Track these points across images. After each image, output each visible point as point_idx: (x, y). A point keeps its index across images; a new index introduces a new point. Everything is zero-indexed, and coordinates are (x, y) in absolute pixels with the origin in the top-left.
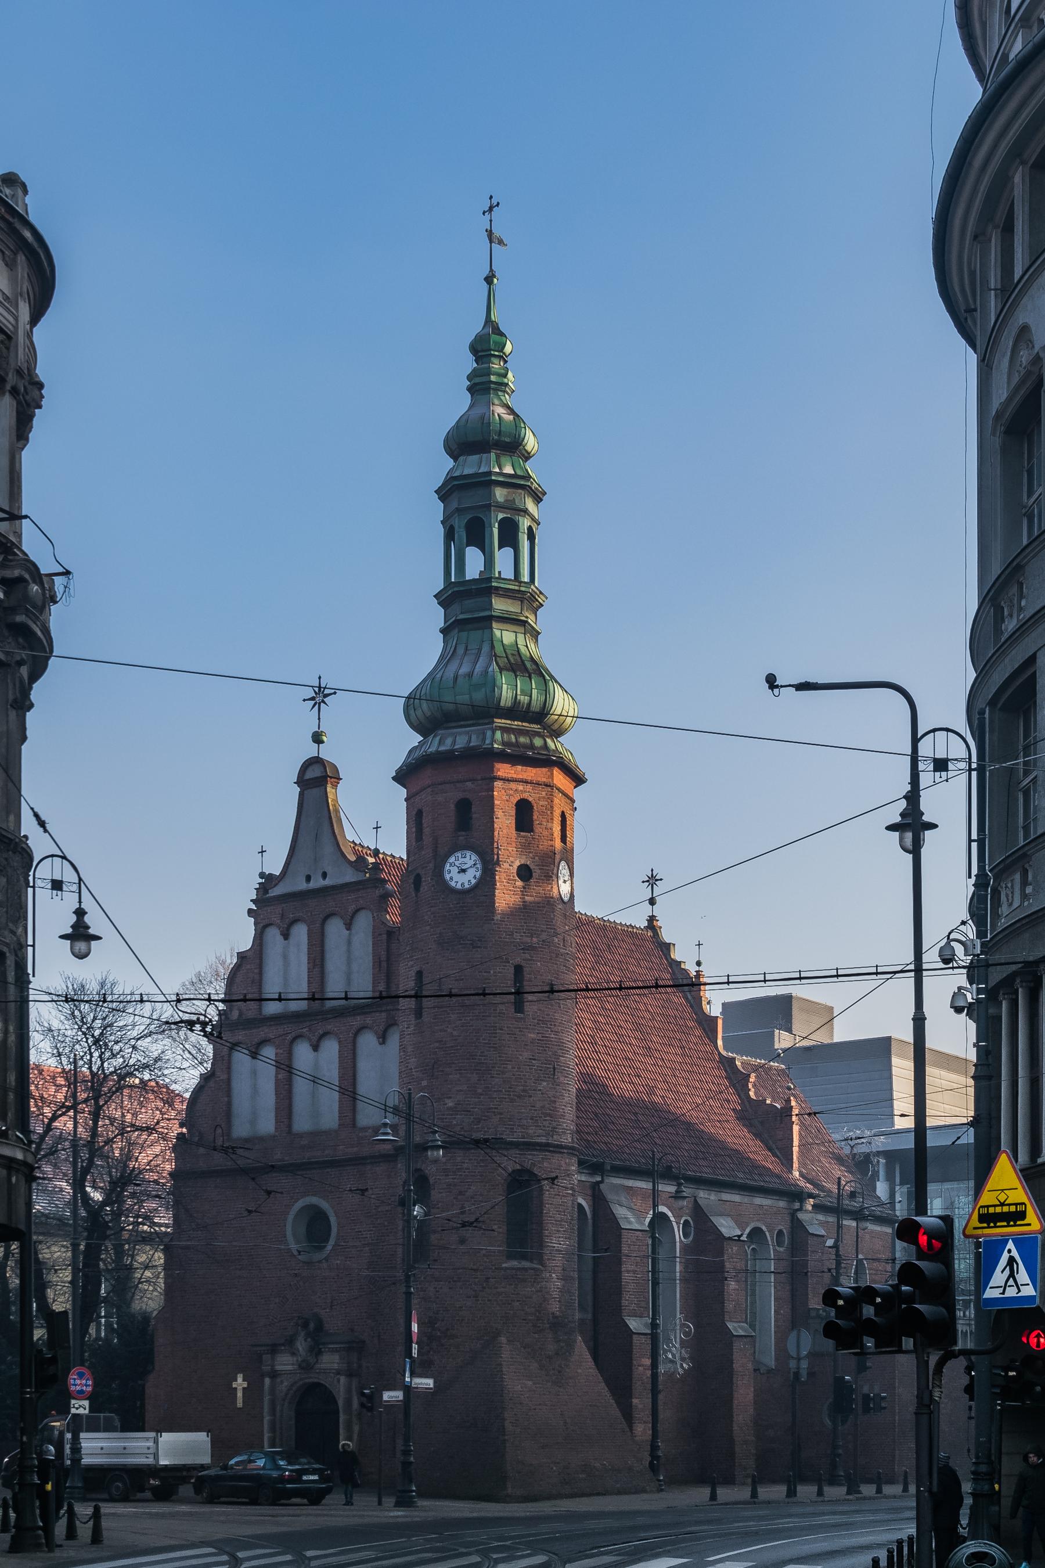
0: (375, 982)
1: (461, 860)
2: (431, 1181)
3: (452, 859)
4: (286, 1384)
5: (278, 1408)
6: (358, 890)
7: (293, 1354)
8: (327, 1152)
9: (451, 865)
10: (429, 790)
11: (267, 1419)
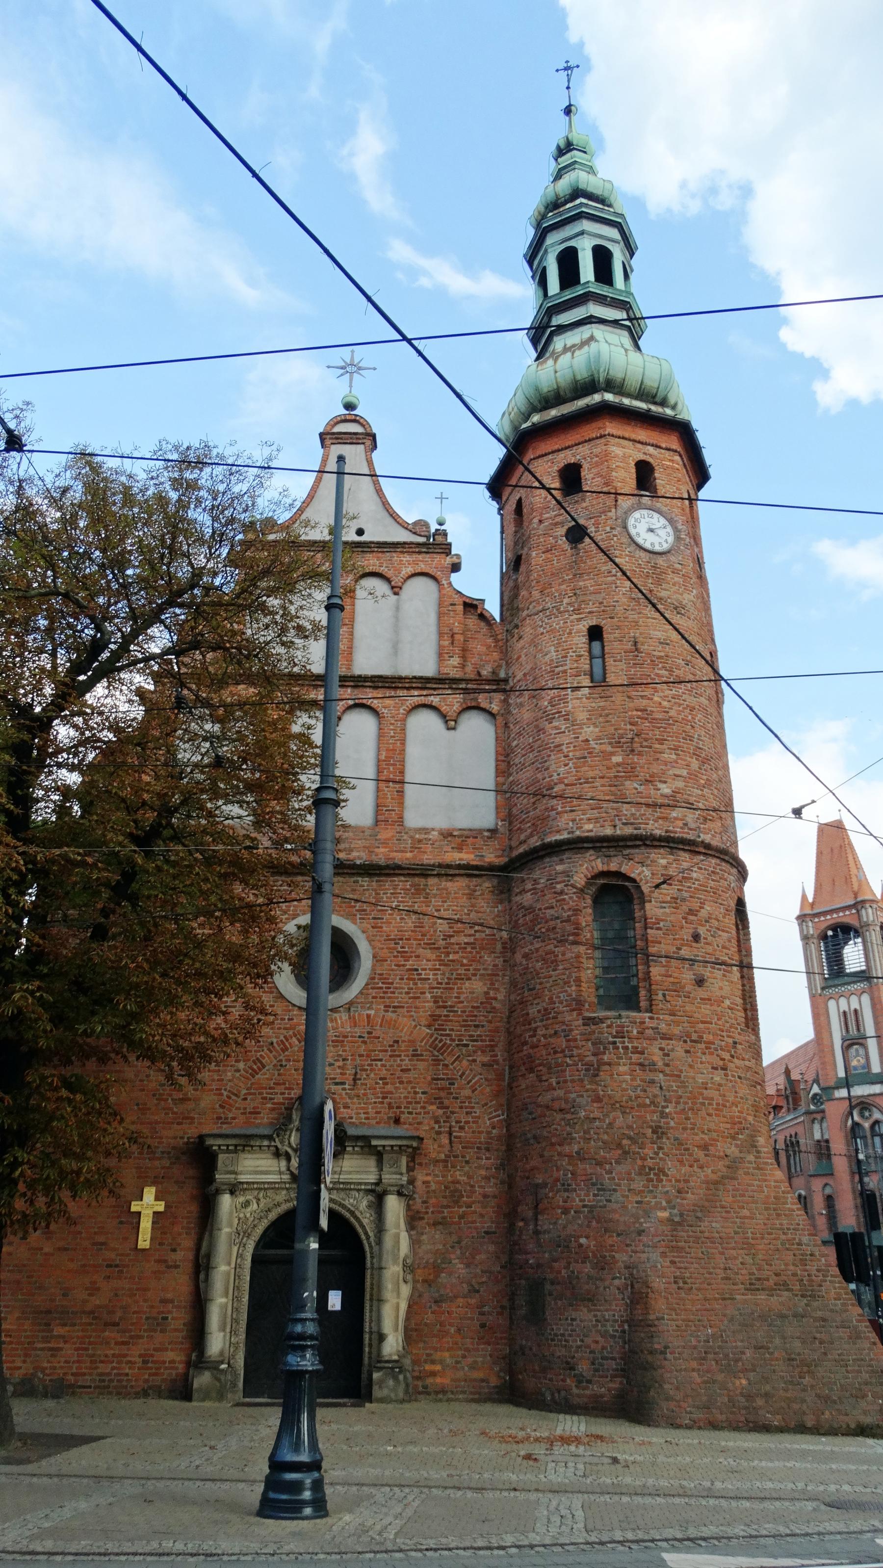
0: (441, 655)
1: (647, 519)
3: (637, 514)
6: (420, 553)
7: (277, 1154)
8: (355, 854)
9: (636, 520)
10: (603, 440)
11: (223, 1268)
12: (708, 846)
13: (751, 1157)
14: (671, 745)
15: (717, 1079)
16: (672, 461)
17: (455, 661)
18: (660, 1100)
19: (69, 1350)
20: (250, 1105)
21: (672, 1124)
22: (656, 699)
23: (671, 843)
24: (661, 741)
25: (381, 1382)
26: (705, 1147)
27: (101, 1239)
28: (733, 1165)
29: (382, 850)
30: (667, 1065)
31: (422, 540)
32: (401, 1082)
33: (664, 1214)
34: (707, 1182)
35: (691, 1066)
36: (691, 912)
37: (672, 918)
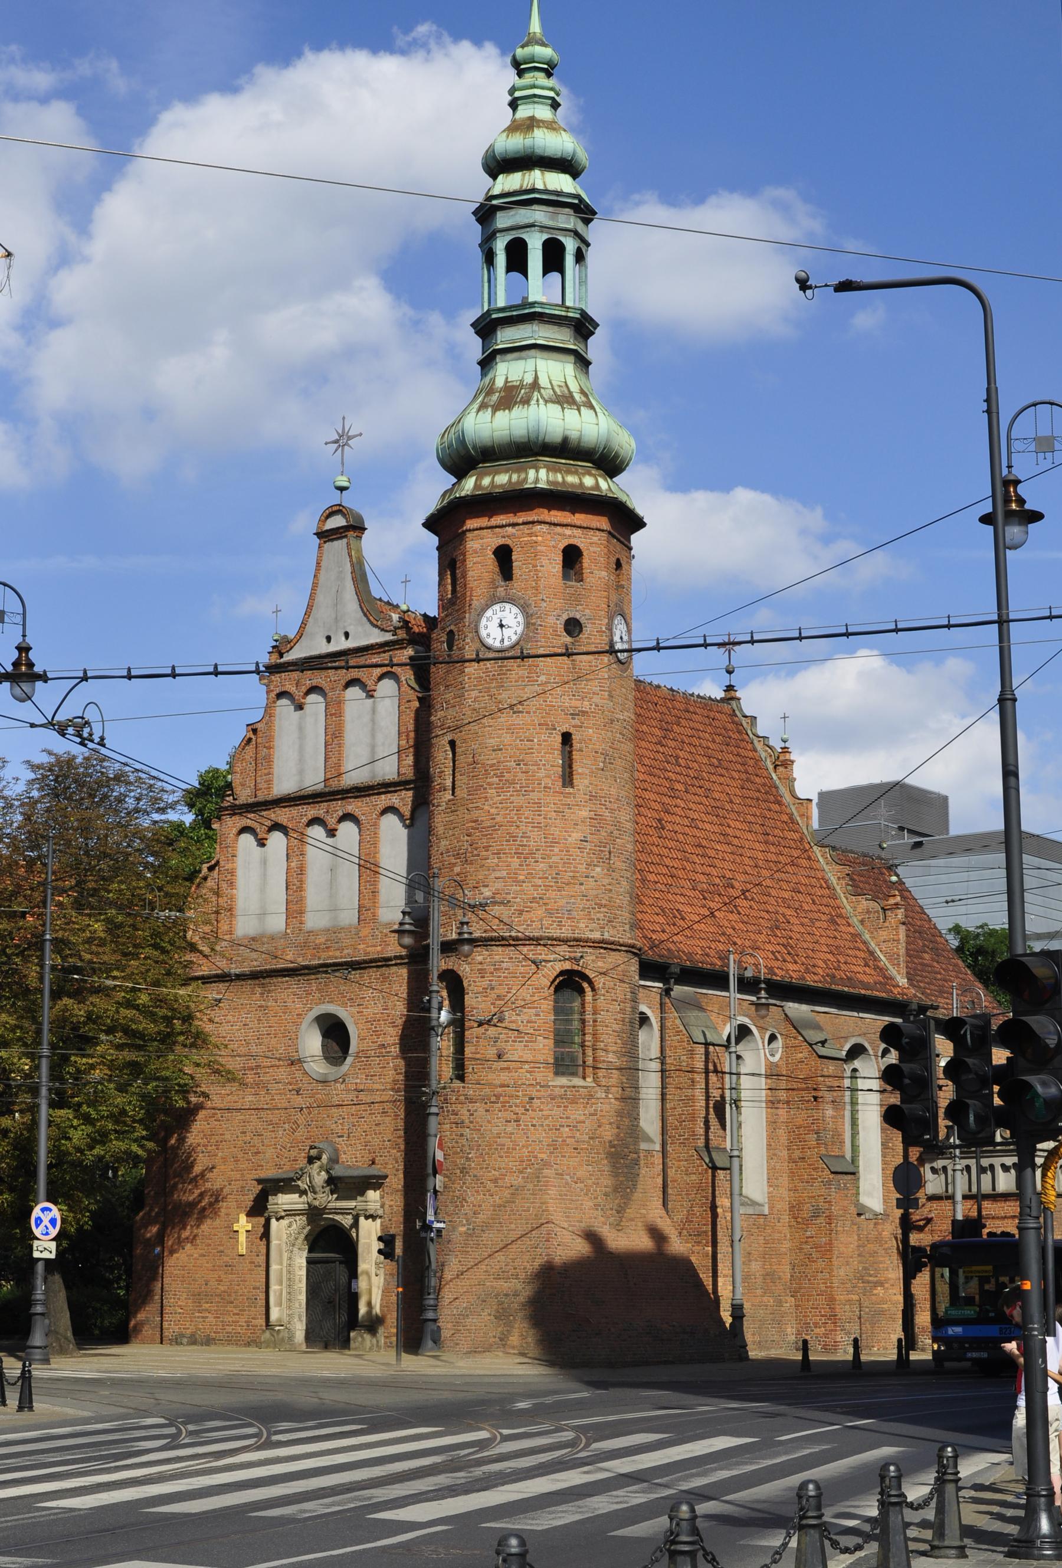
1: (500, 615)
2: (465, 984)
3: (489, 613)
4: (294, 1226)
5: (285, 1255)
8: (346, 952)
12: (516, 939)
13: (530, 1186)
14: (494, 849)
15: (509, 1129)
16: (530, 535)
17: (410, 760)
18: (466, 1148)
19: (211, 1318)
20: (293, 1154)
21: (473, 1165)
22: (486, 807)
23: (486, 942)
24: (487, 848)
25: (355, 1338)
26: (495, 1181)
27: (222, 1248)
28: (516, 1191)
29: (362, 946)
30: (471, 1122)
31: (388, 637)
32: (375, 1134)
33: (463, 1229)
34: (494, 1206)
35: (489, 1122)
36: (499, 997)
37: (483, 1006)
